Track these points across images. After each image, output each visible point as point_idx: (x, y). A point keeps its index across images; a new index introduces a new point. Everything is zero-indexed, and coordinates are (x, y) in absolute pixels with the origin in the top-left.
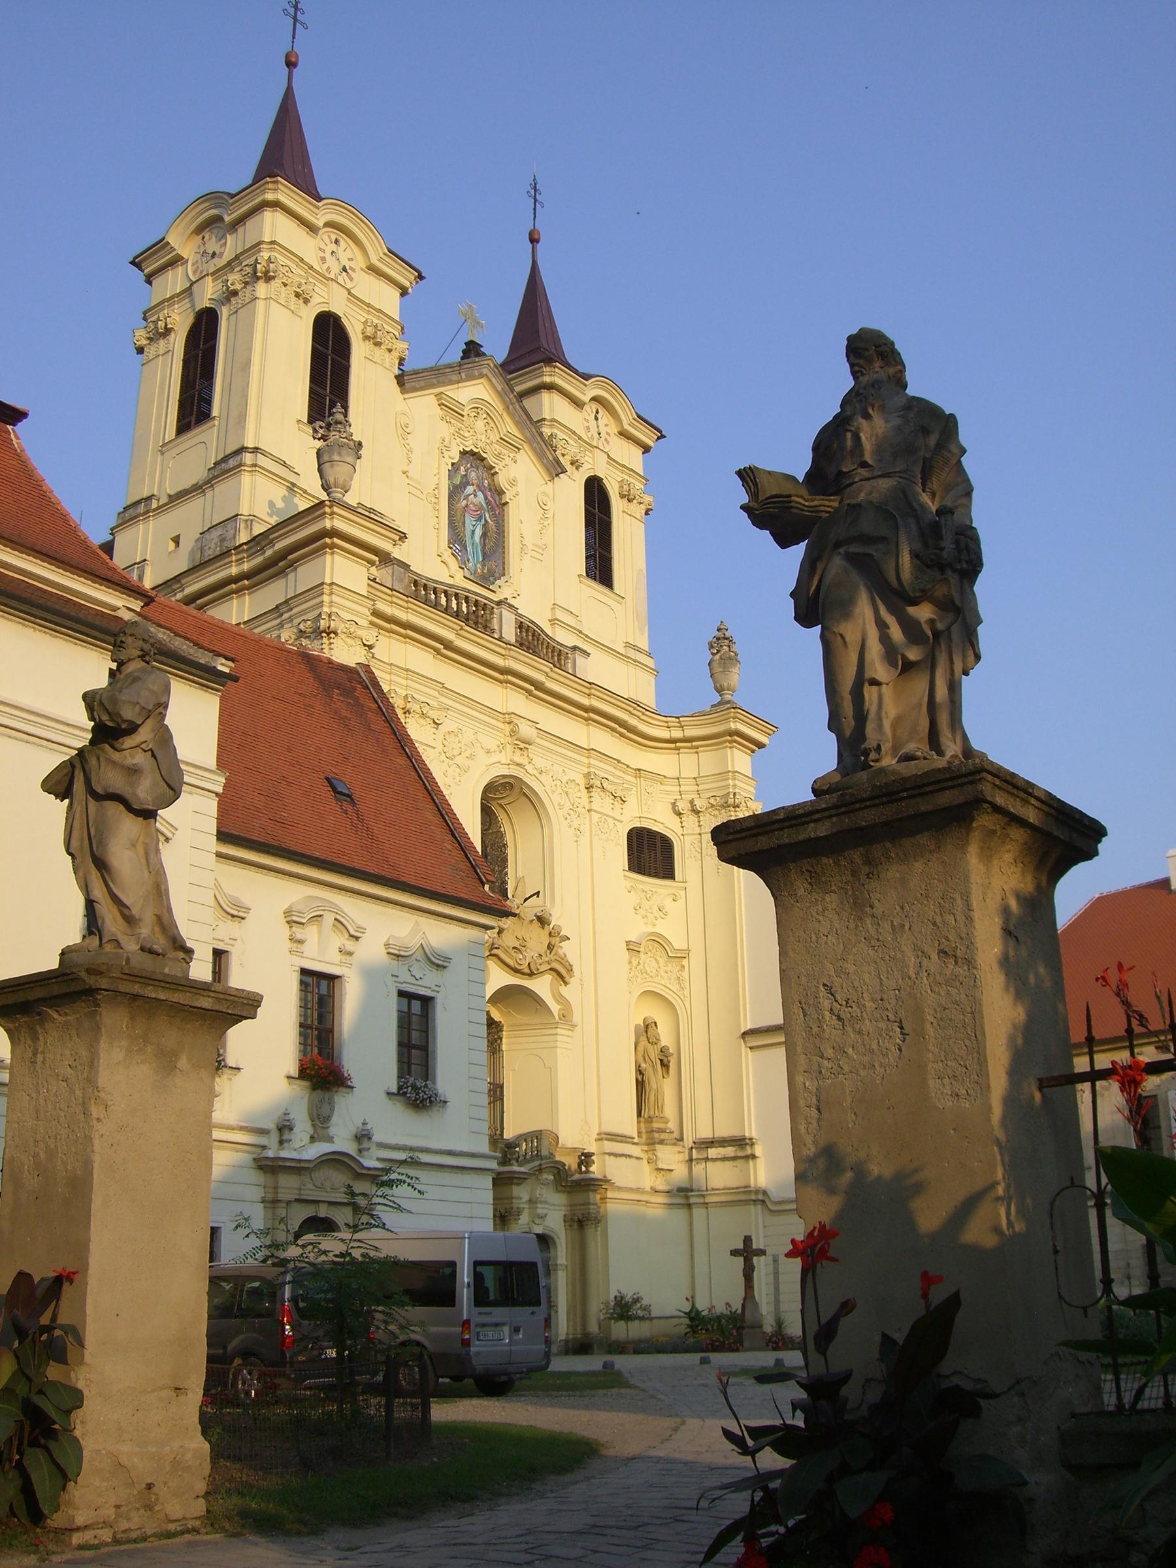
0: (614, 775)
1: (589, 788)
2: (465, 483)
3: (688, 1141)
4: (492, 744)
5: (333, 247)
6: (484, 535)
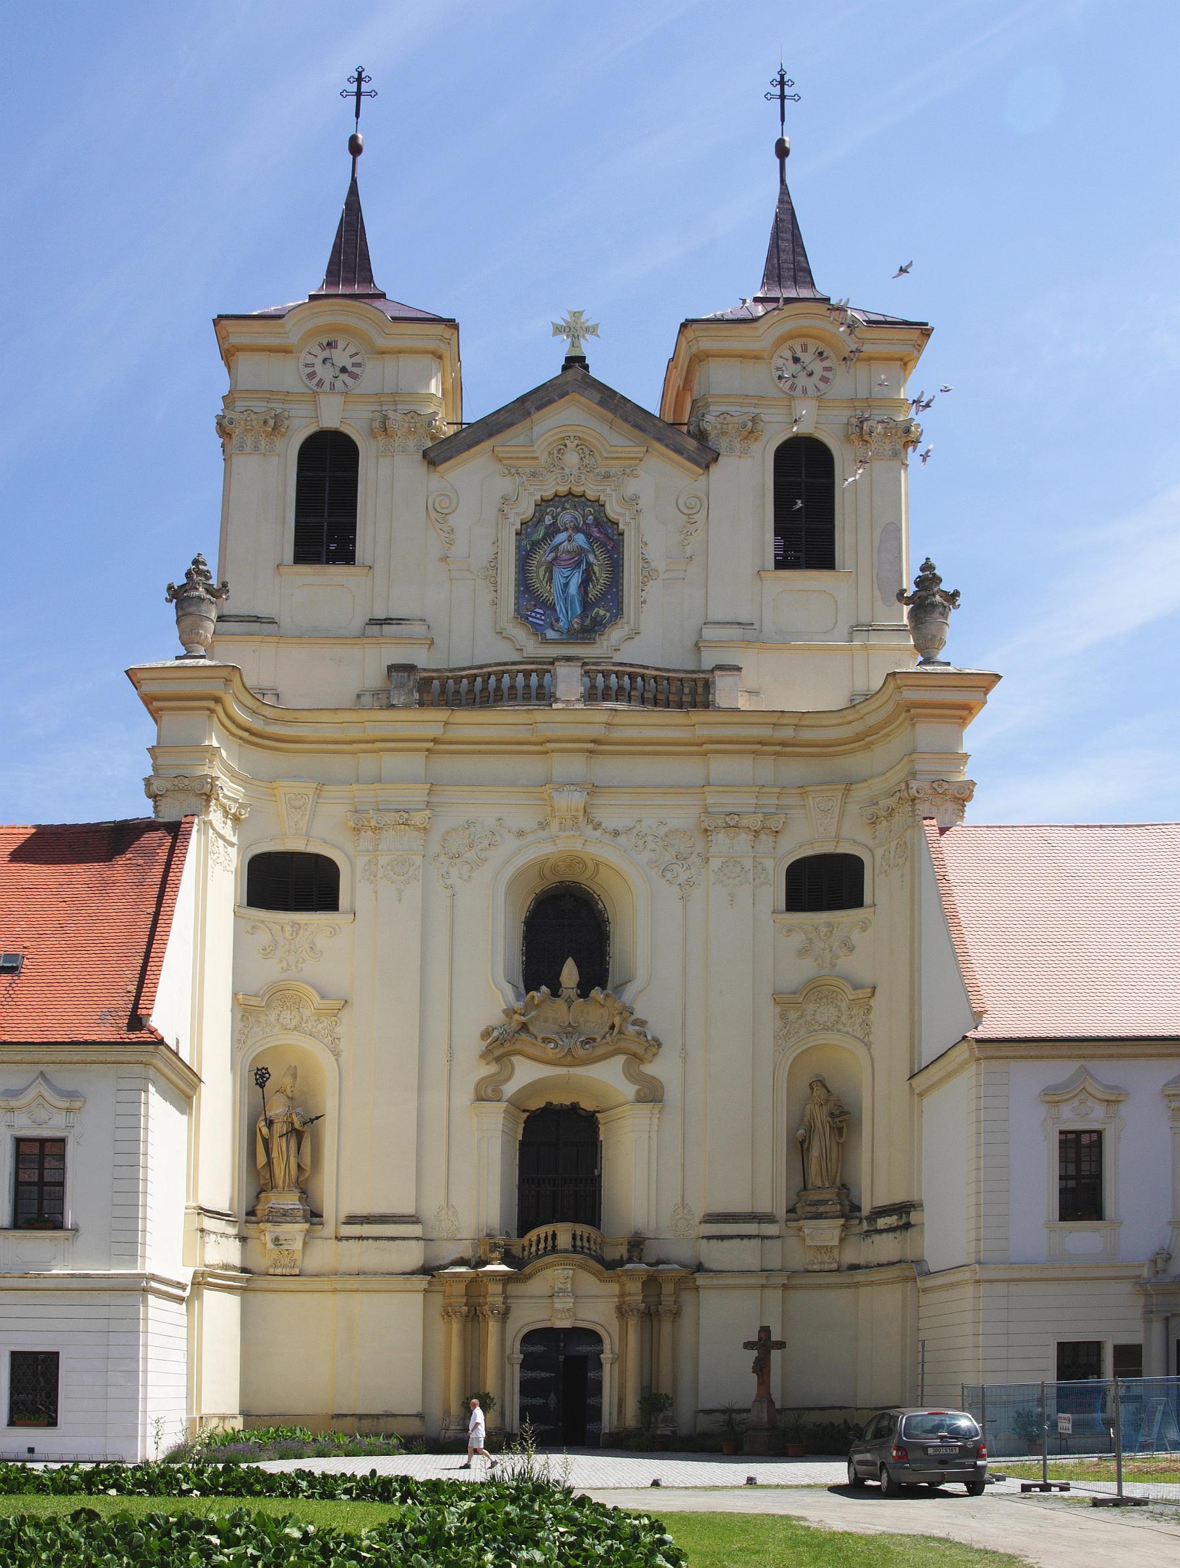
2: (553, 530)
5: (326, 354)
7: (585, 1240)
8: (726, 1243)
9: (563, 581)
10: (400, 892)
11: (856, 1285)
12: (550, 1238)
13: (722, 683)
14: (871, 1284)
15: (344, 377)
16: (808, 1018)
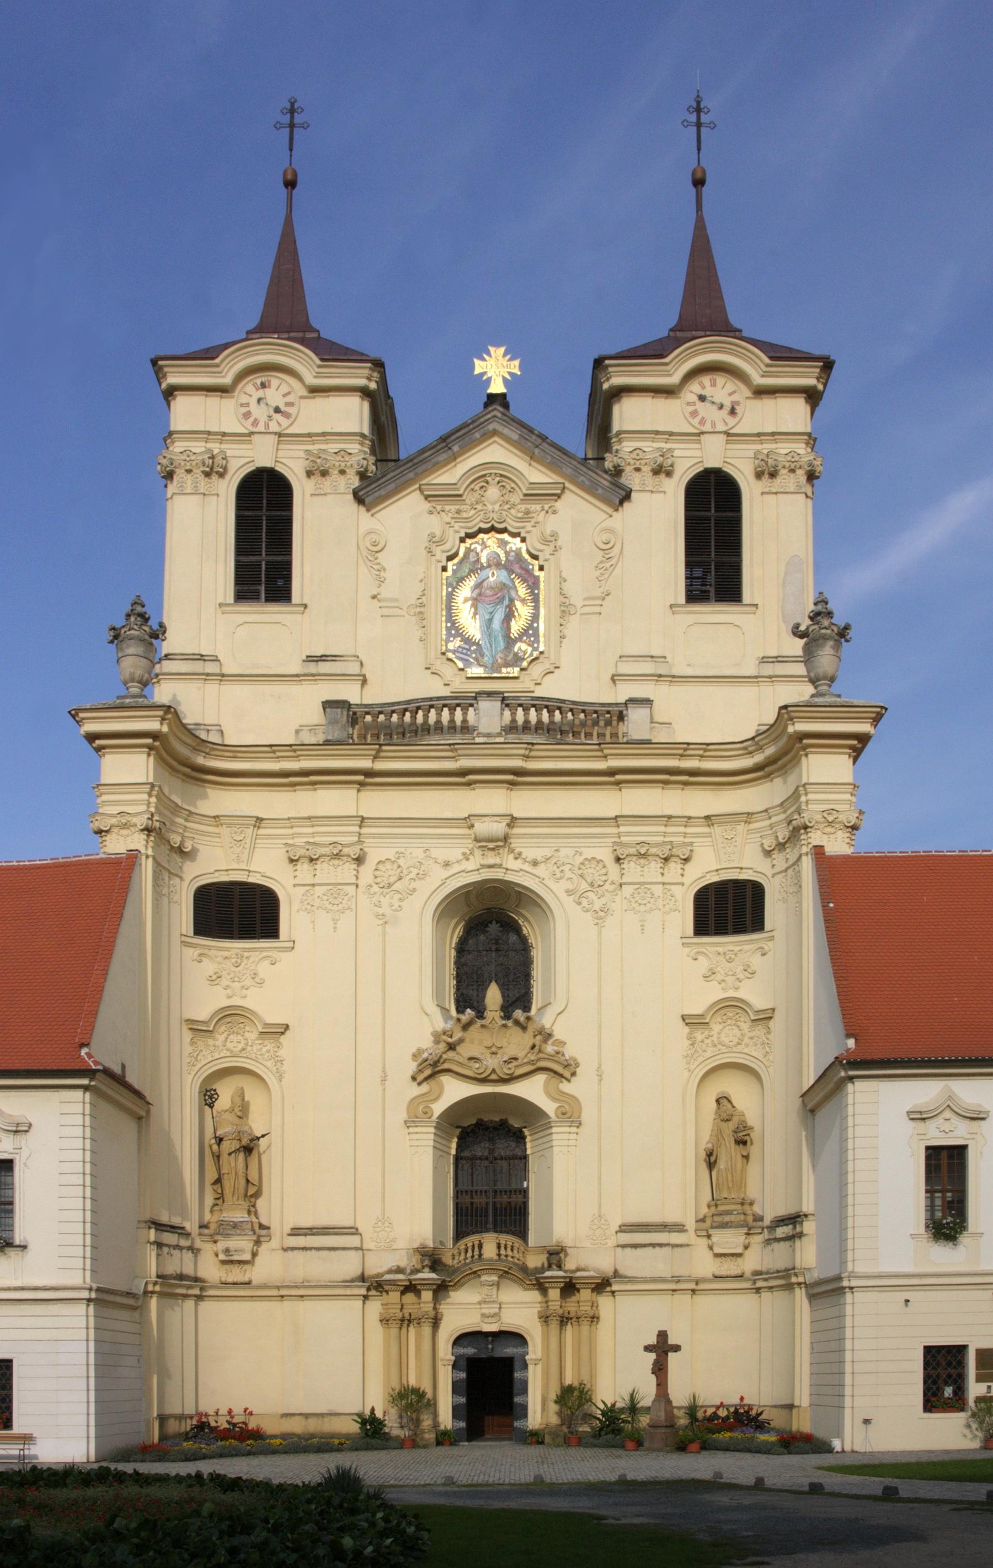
0: (657, 834)
1: (618, 860)
4: (454, 853)
8: (639, 1251)
9: (487, 617)
10: (335, 921)
12: (476, 1249)
13: (636, 716)
15: (278, 417)
16: (715, 1039)
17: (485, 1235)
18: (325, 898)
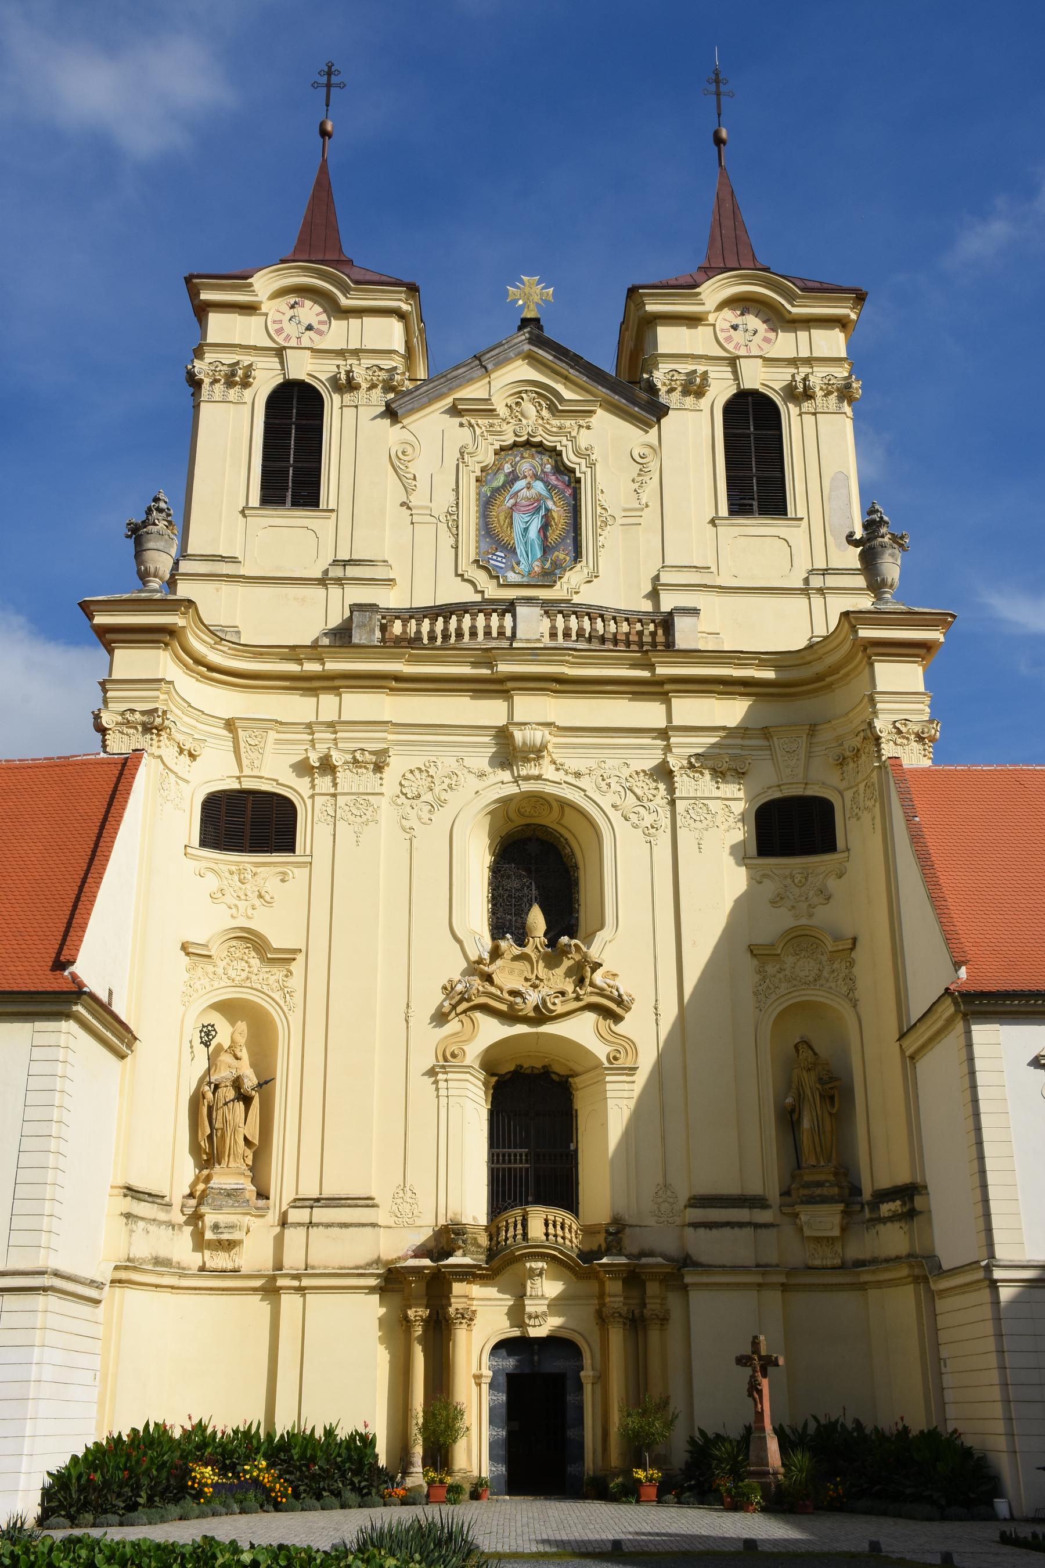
2: (513, 478)
3: (867, 1195)
6: (545, 528)
7: (558, 1228)
8: (715, 1233)
9: (524, 526)
11: (863, 1287)
12: (519, 1226)
13: (681, 623)
14: (879, 1284)
16: (787, 972)
17: (530, 1209)
18: (347, 808)
